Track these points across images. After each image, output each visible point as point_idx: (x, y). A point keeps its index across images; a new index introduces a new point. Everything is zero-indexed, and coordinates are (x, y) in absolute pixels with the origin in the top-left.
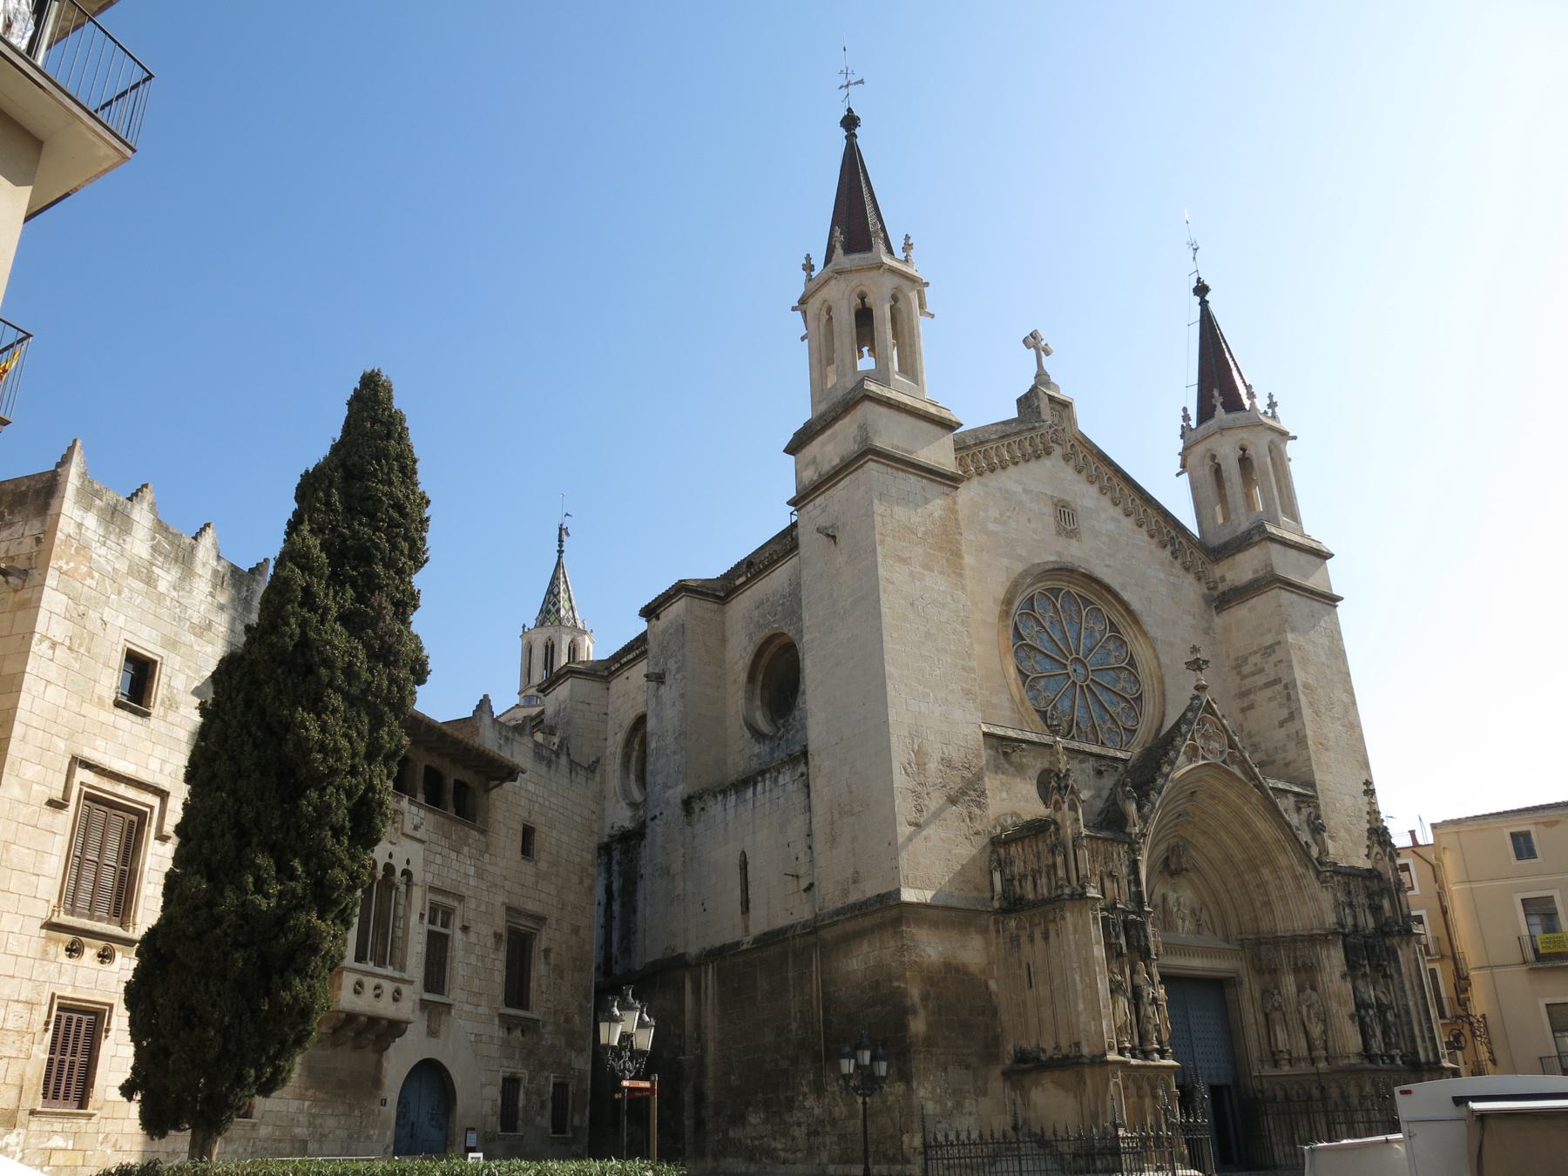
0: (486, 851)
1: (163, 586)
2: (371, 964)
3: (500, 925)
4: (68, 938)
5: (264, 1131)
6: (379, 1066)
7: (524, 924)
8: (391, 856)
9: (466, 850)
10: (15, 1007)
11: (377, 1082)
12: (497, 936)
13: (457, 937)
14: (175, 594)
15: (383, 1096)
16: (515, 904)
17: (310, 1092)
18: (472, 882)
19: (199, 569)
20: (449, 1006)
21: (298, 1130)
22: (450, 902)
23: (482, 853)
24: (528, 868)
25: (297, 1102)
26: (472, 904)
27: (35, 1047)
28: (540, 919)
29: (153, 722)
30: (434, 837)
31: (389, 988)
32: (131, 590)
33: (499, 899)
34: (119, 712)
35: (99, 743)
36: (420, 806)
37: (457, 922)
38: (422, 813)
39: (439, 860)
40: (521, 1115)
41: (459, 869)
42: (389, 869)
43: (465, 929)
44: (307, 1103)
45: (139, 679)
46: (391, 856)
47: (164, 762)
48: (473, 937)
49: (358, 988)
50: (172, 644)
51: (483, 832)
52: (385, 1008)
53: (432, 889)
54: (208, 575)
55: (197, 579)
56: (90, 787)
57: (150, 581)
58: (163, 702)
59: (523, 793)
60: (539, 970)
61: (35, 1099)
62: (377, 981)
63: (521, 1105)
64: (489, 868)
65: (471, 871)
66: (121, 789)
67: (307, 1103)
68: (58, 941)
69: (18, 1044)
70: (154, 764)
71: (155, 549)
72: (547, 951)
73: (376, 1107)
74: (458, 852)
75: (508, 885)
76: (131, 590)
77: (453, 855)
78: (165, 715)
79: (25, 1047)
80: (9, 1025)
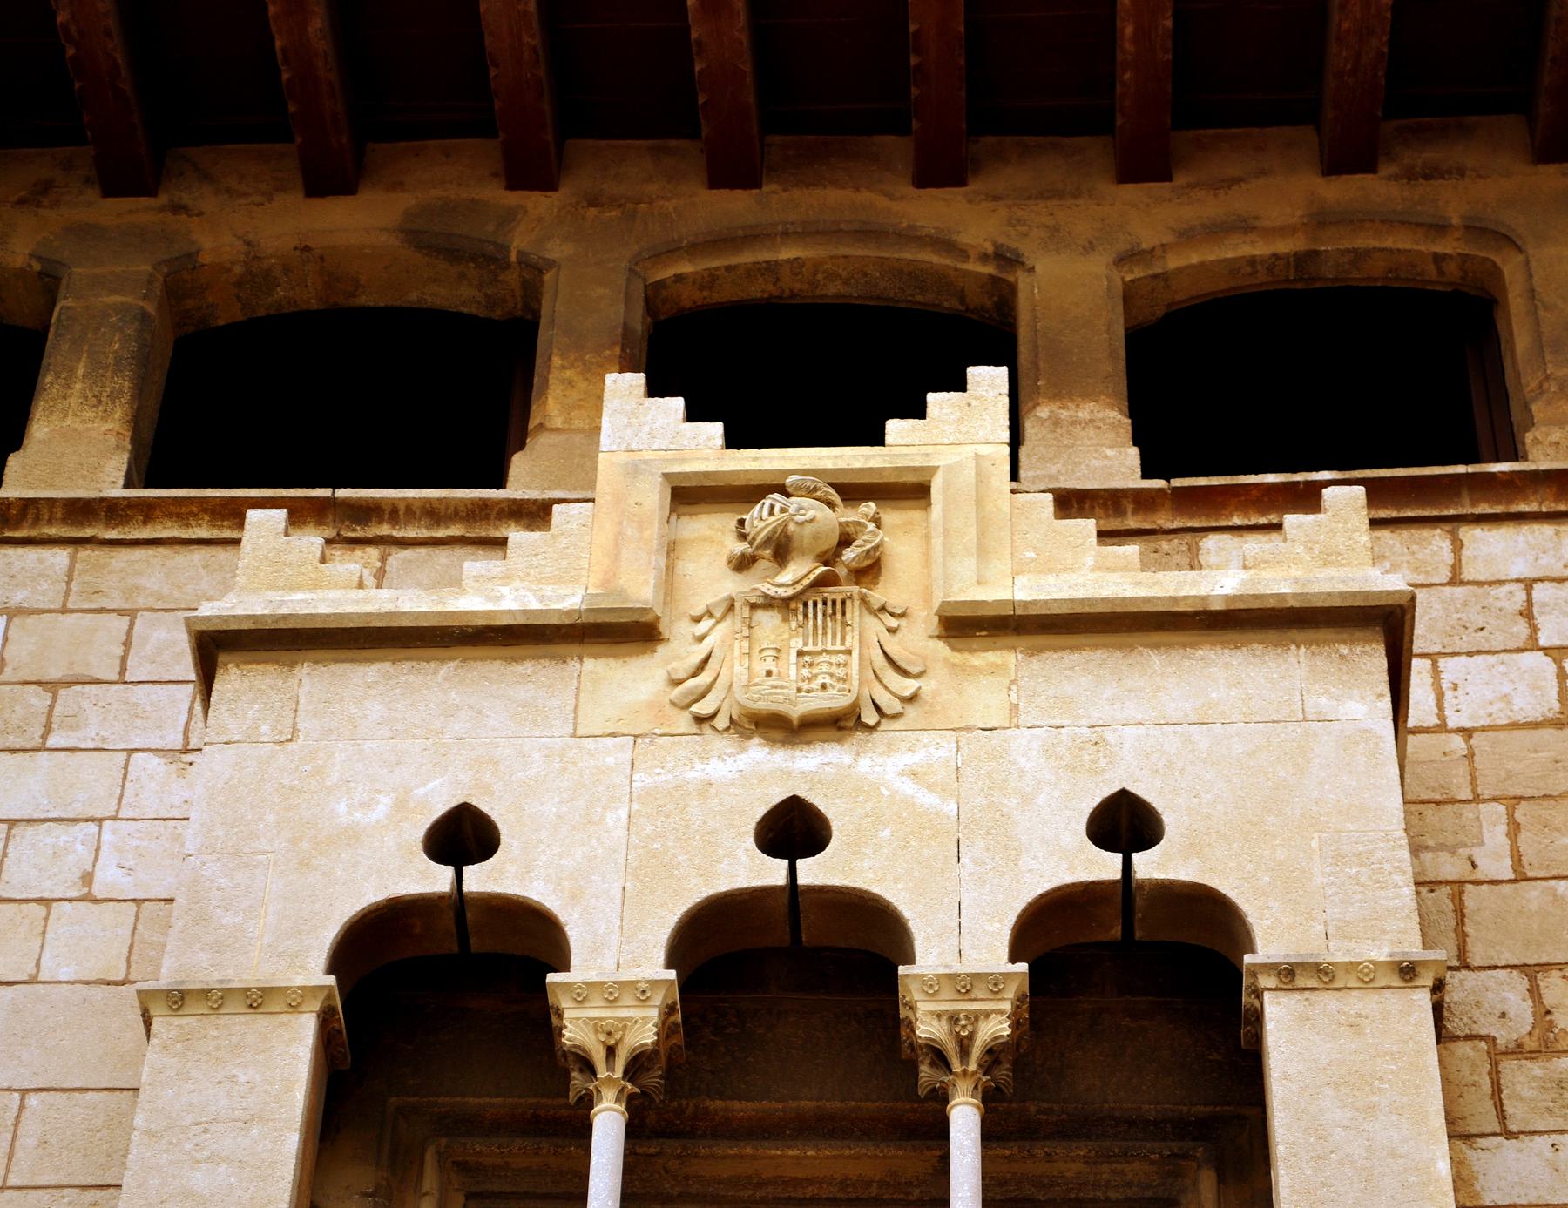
42: (788, 965)
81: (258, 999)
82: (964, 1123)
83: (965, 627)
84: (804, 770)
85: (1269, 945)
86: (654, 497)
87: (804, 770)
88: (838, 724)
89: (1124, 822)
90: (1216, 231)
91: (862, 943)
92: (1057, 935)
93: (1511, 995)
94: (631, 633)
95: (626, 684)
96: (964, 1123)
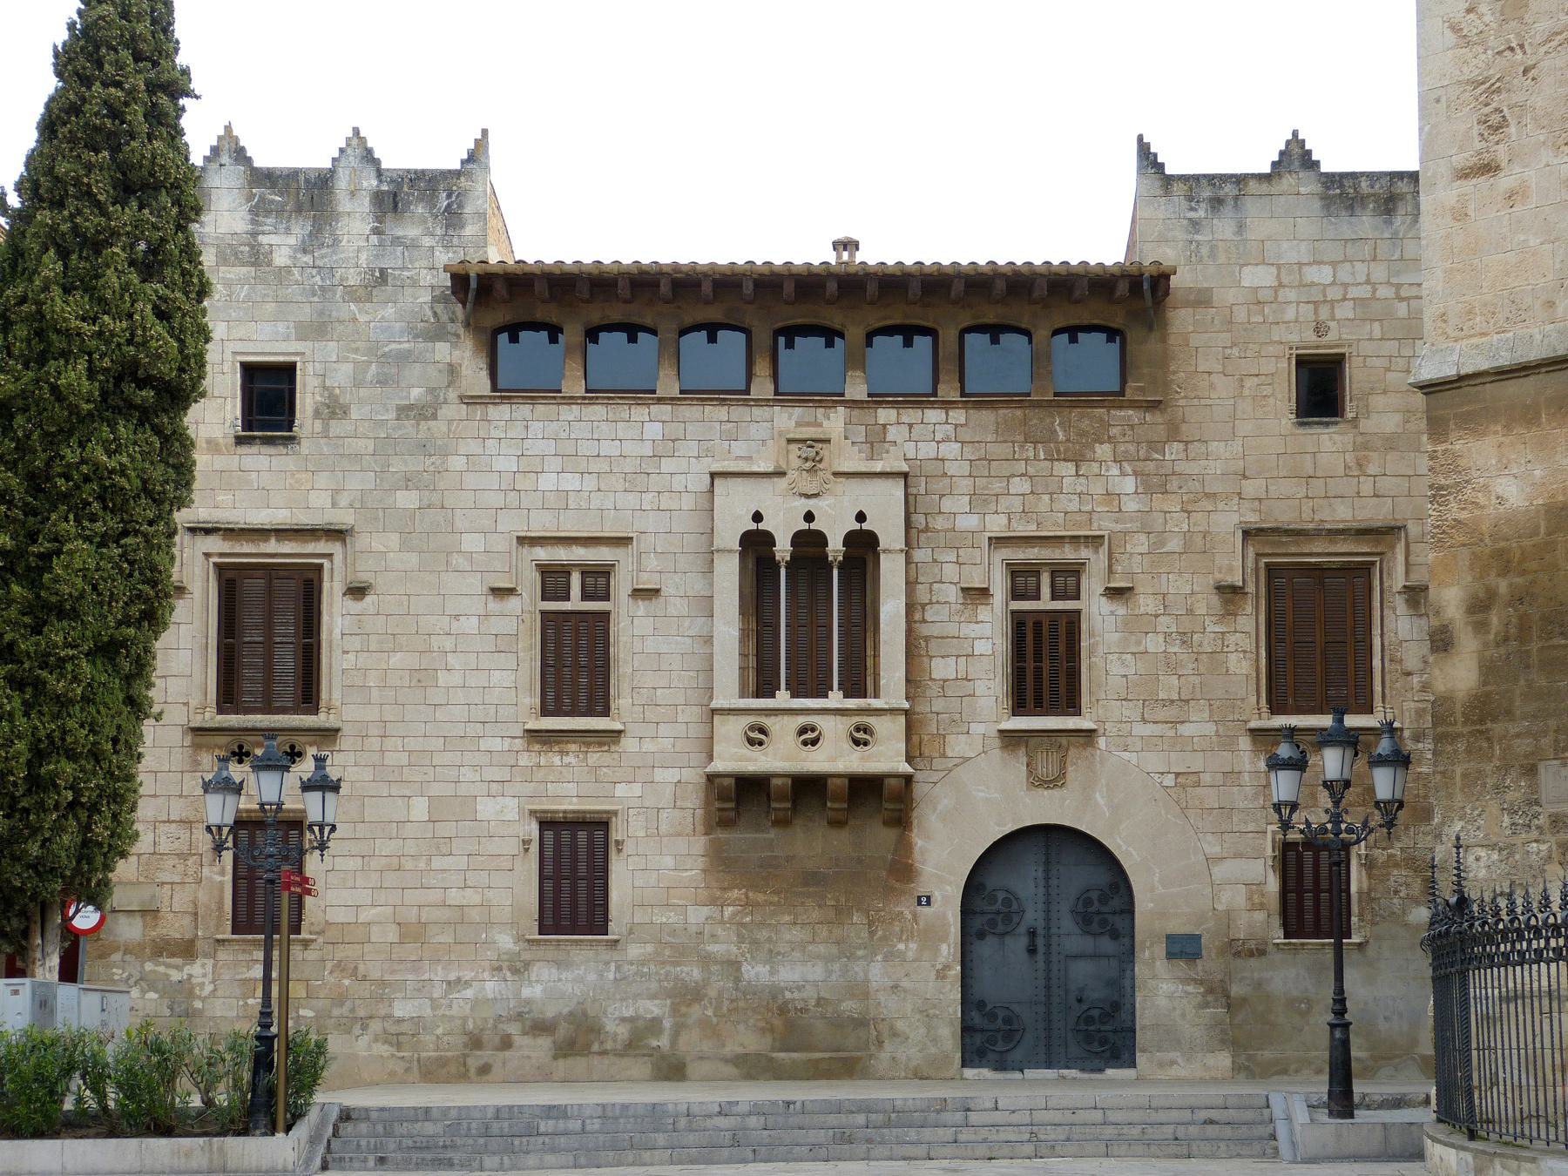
0: (1174, 433)
1: (281, 258)
2: (783, 698)
3: (1234, 564)
4: (223, 740)
5: (634, 951)
6: (904, 847)
7: (1318, 552)
8: (809, 517)
9: (1103, 450)
10: (162, 828)
11: (903, 870)
12: (1230, 593)
13: (1096, 610)
14: (307, 259)
15: (922, 891)
16: (1284, 516)
17: (735, 893)
18: (1131, 505)
19: (344, 204)
20: (1089, 734)
21: (712, 948)
22: (1068, 554)
23: (1155, 446)
24: (1329, 440)
25: (705, 911)
26: (1140, 544)
27: (206, 871)
28: (1386, 533)
29: (305, 447)
30: (1003, 450)
31: (834, 730)
32: (228, 284)
33: (1228, 521)
34: (244, 449)
35: (222, 497)
36: (947, 405)
37: (1093, 585)
38: (958, 416)
39: (1020, 486)
40: (1355, 908)
41: (1090, 489)
42: (809, 541)
43: (1115, 593)
44: (729, 911)
45: (269, 398)
46: (809, 517)
47: (336, 492)
48: (1146, 603)
49: (757, 737)
50: (317, 330)
51: (1154, 406)
52: (834, 757)
53: (997, 542)
54: (364, 204)
55: (344, 221)
56: (221, 555)
57: (257, 257)
58: (317, 414)
59: (1291, 295)
60: (1397, 630)
61: (219, 926)
62: (802, 720)
63: (1354, 888)
64: (1181, 467)
65: (1129, 484)
66: (272, 546)
67: (729, 911)
68: (209, 748)
69: (180, 868)
70: (320, 499)
71: (259, 211)
72: (1415, 595)
73: (906, 908)
74: (1078, 460)
75: (1251, 488)
76: (228, 284)
77: (1070, 468)
78: (326, 429)
79: (191, 871)
80: (162, 849)
81: (730, 551)
82: (835, 572)
83: (836, 474)
84: (811, 505)
85: (882, 546)
86: (784, 442)
87: (811, 505)
88: (816, 495)
89: (861, 517)
90: (885, 318)
91: (819, 539)
92: (851, 539)
93: (922, 519)
94: (782, 474)
95: (782, 483)
96: (835, 572)
